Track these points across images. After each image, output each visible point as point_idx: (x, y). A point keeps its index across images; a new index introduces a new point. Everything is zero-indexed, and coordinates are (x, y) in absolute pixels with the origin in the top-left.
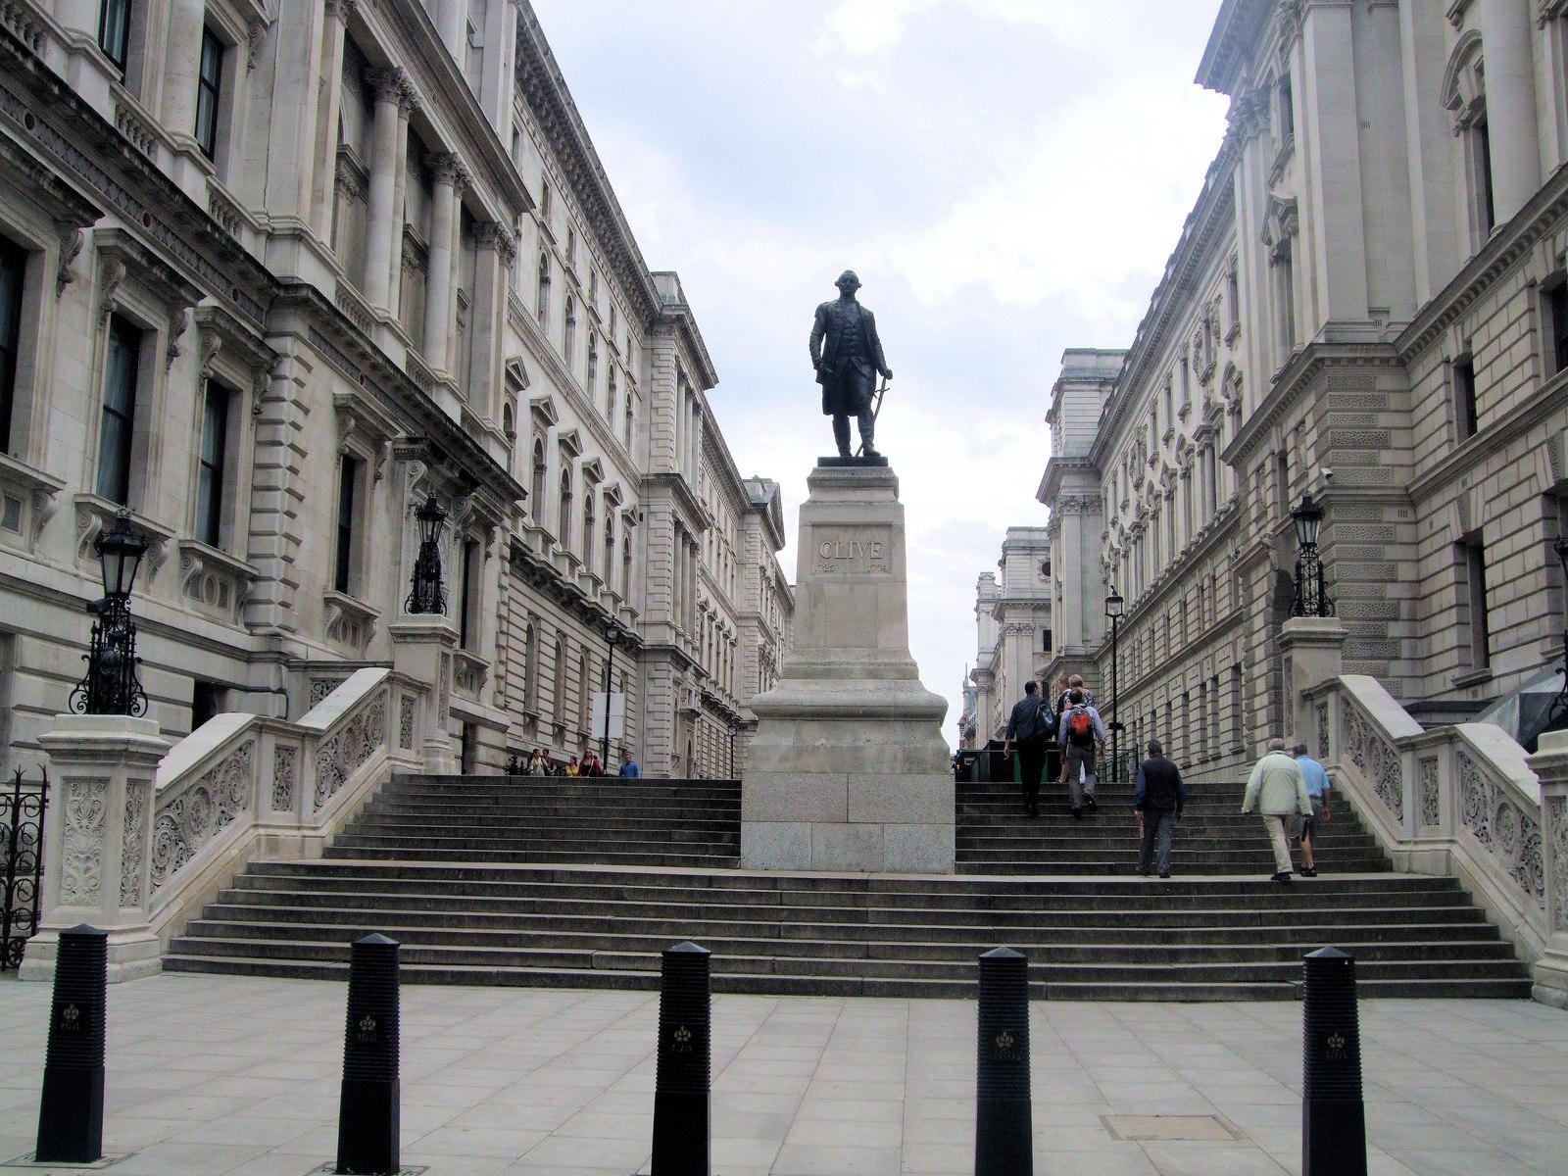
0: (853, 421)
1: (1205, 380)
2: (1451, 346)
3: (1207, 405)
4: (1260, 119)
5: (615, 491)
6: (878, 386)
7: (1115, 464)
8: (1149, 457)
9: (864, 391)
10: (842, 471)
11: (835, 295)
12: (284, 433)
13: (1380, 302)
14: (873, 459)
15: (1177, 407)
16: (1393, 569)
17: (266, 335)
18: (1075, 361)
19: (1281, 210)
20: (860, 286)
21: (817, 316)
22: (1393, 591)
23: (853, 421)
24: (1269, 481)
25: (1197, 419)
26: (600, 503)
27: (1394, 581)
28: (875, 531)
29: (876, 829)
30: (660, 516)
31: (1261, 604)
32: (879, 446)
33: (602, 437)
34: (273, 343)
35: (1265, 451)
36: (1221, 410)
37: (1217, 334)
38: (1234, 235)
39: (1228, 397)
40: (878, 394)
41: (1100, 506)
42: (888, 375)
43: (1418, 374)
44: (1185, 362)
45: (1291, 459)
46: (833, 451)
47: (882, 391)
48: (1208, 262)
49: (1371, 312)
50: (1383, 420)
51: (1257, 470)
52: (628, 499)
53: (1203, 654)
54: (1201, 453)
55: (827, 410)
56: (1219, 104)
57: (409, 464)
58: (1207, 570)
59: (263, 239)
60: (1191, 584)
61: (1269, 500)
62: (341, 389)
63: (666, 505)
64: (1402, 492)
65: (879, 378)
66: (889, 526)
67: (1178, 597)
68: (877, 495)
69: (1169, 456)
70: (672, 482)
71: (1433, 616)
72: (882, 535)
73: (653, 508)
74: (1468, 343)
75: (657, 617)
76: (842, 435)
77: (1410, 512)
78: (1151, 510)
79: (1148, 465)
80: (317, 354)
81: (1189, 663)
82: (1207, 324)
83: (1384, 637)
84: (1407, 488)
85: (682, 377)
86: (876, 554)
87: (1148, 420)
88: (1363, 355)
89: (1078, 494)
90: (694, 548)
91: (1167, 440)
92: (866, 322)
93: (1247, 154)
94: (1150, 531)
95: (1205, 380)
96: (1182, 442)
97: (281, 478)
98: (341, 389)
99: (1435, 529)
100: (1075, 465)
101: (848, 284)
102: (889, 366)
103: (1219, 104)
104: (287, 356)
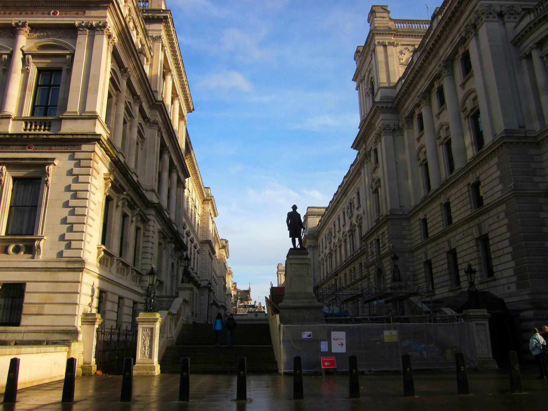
0: (297, 239)
1: (350, 218)
2: (421, 216)
4: (369, 158)
7: (322, 236)
11: (292, 210)
12: (150, 239)
18: (310, 210)
19: (375, 181)
22: (409, 274)
23: (297, 239)
24: (374, 246)
25: (347, 228)
26: (193, 248)
31: (373, 276)
34: (148, 217)
35: (373, 238)
36: (355, 225)
37: (354, 206)
43: (412, 222)
44: (344, 213)
45: (380, 241)
46: (293, 247)
48: (351, 188)
49: (400, 207)
50: (404, 232)
52: (198, 247)
54: (349, 236)
56: (356, 152)
57: (170, 244)
58: (352, 266)
60: (347, 269)
61: (374, 250)
63: (207, 248)
66: (308, 264)
67: (344, 272)
68: (304, 257)
74: (426, 215)
75: (204, 278)
76: (294, 242)
82: (351, 204)
87: (333, 226)
93: (365, 166)
94: (334, 254)
95: (350, 218)
96: (344, 233)
97: (149, 250)
98: (159, 227)
101: (295, 207)
103: (356, 152)
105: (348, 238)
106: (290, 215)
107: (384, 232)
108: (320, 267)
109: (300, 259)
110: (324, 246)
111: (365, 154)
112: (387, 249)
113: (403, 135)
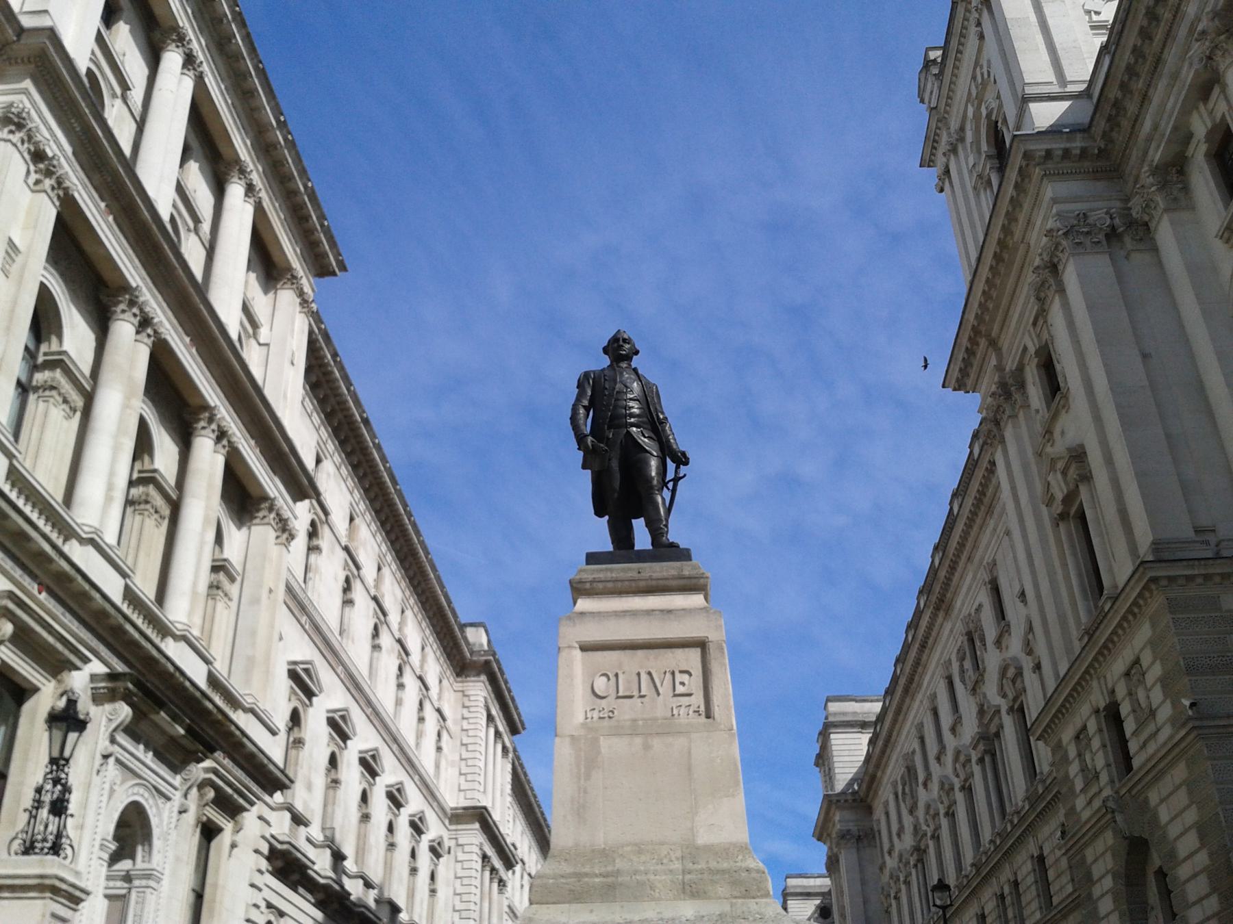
0: (639, 525)
3: (981, 712)
4: (1017, 396)
5: (420, 819)
6: (670, 475)
7: (885, 794)
10: (623, 570)
13: (1204, 522)
19: (1060, 465)
21: (580, 385)
24: (1096, 743)
25: (970, 728)
28: (679, 652)
30: (467, 849)
32: (676, 533)
33: (408, 763)
36: (998, 711)
37: (983, 640)
38: (1004, 509)
39: (1004, 696)
40: (670, 485)
41: (874, 837)
45: (1125, 709)
47: (676, 480)
49: (1198, 531)
52: (435, 829)
54: (981, 761)
57: (108, 707)
58: (1006, 874)
61: (1100, 762)
63: (473, 836)
70: (481, 817)
73: (461, 841)
79: (921, 788)
85: (490, 718)
87: (916, 745)
88: (1203, 572)
89: (853, 827)
90: (502, 883)
93: (1009, 433)
100: (846, 801)
105: (977, 769)
108: (888, 912)
109: (649, 613)
110: (895, 827)
111: (1003, 385)
112: (1166, 732)
113: (1155, 250)
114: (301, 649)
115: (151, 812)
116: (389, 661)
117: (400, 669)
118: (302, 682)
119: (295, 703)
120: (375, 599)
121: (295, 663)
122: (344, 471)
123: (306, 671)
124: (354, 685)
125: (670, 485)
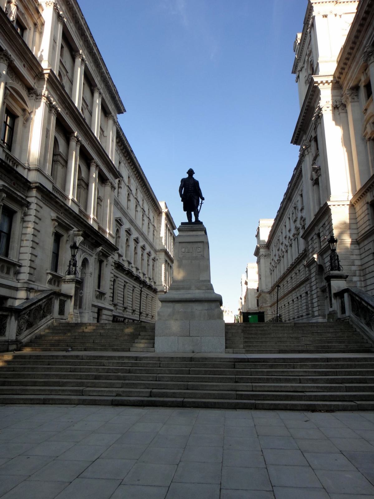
0: (193, 213)
1: (295, 221)
6: (200, 202)
8: (281, 243)
9: (195, 204)
11: (186, 176)
14: (198, 222)
15: (288, 229)
16: (353, 262)
17: (27, 197)
20: (194, 173)
22: (354, 268)
23: (193, 213)
25: (293, 231)
27: (354, 265)
29: (199, 338)
30: (162, 259)
31: (314, 274)
32: (200, 219)
33: (146, 239)
34: (29, 200)
35: (314, 233)
37: (298, 210)
39: (301, 225)
42: (203, 199)
44: (289, 218)
46: (186, 220)
47: (202, 204)
48: (295, 192)
51: (311, 239)
53: (297, 290)
54: (295, 240)
55: (185, 210)
56: (297, 149)
58: (298, 268)
59: (26, 170)
62: (54, 215)
64: (355, 241)
65: (200, 200)
69: (286, 242)
71: (366, 274)
72: (200, 245)
73: (160, 257)
76: (189, 217)
77: (357, 246)
78: (281, 256)
80: (44, 203)
81: (293, 292)
83: (352, 281)
84: (356, 239)
86: (199, 251)
89: (264, 253)
91: (286, 237)
92: (196, 183)
98: (54, 215)
99: (366, 250)
101: (191, 172)
102: (203, 196)
104: (33, 203)
106: (183, 181)
107: (324, 224)
108: (271, 274)
109: (193, 236)
113: (346, 112)
114: (119, 215)
115: (89, 259)
116: (140, 214)
117: (143, 215)
118: (119, 222)
119: (117, 228)
120: (136, 198)
121: (117, 218)
122: (126, 165)
123: (120, 220)
124: (131, 222)
125: (200, 205)
